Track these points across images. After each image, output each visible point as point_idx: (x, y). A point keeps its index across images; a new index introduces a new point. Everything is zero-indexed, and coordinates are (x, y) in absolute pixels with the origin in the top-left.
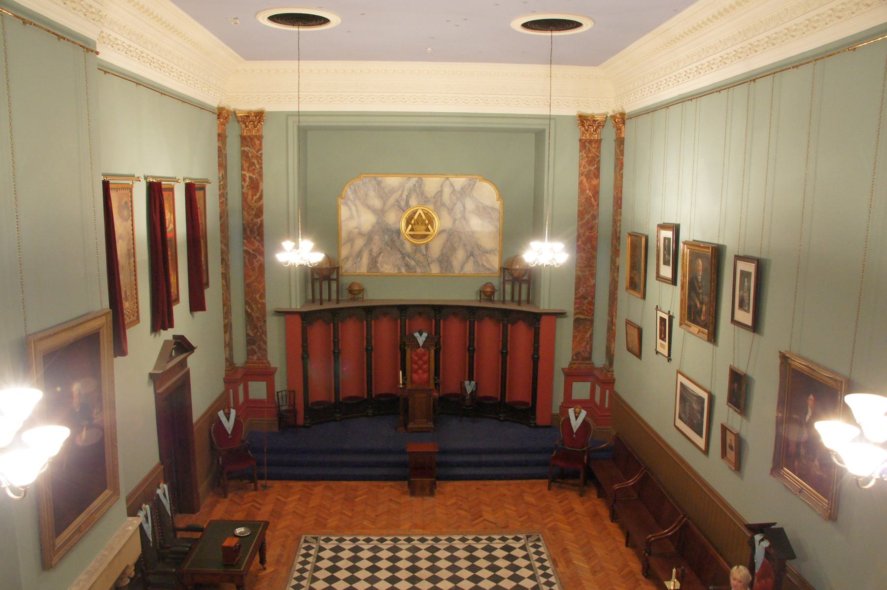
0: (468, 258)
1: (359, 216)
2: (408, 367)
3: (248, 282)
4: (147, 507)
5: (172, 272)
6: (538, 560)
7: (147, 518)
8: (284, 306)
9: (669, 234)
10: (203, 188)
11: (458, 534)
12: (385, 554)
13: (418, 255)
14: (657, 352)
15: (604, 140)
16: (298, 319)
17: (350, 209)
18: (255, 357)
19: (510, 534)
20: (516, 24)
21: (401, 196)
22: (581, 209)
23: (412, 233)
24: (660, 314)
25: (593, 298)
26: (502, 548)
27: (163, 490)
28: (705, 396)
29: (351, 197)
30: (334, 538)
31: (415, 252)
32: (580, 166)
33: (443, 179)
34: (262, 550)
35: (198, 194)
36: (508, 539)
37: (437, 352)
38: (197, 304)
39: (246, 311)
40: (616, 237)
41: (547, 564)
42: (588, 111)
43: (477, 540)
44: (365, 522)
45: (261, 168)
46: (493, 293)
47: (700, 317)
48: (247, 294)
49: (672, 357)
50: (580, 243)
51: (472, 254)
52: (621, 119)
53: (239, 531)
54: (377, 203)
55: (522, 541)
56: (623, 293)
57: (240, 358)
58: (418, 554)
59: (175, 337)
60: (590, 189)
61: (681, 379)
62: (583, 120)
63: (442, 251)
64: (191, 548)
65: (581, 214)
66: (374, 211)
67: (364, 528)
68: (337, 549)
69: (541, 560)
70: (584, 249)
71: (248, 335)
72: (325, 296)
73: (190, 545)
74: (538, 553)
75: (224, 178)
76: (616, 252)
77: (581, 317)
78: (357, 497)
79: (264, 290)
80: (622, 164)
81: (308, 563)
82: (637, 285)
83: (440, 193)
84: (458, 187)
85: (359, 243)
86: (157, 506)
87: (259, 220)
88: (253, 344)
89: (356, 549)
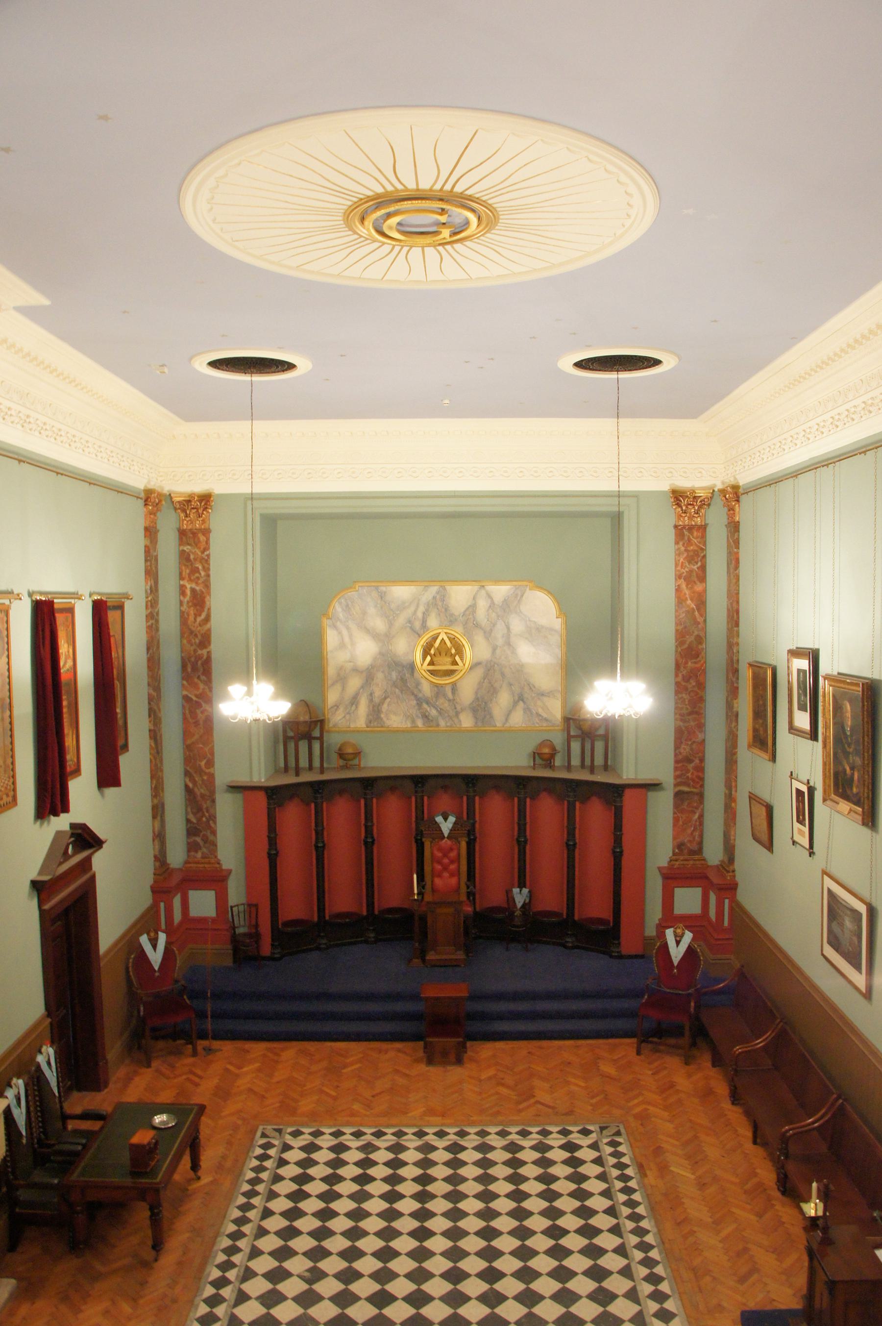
0: (515, 704)
1: (353, 644)
2: (427, 869)
3: (189, 742)
4: (21, 1082)
5: (68, 730)
6: (616, 1166)
7: (18, 1099)
8: (243, 779)
9: (803, 664)
10: (120, 607)
11: (496, 1125)
12: (382, 1156)
14: (794, 843)
15: (709, 526)
16: (262, 796)
17: (340, 633)
18: (199, 855)
19: (575, 1124)
20: (566, 363)
21: (415, 612)
22: (680, 628)
23: (431, 668)
24: (796, 785)
25: (702, 760)
26: (562, 1147)
27: (46, 1057)
28: (862, 909)
29: (341, 616)
30: (307, 1130)
31: (437, 695)
32: (676, 565)
33: (476, 588)
34: (194, 1146)
35: (112, 616)
36: (570, 1132)
37: (471, 845)
38: (108, 776)
39: (186, 786)
40: (733, 670)
41: (629, 1172)
42: (684, 483)
43: (524, 1134)
44: (356, 1106)
45: (208, 576)
46: (552, 756)
47: (852, 789)
48: (188, 760)
49: (815, 850)
50: (680, 679)
52: (733, 495)
53: (158, 1119)
54: (379, 624)
55: (594, 1135)
56: (746, 755)
57: (177, 856)
58: (433, 1156)
59: (73, 826)
60: (692, 600)
61: (829, 883)
62: (678, 496)
63: (476, 693)
64: (84, 1146)
65: (681, 636)
66: (375, 636)
67: (352, 1115)
68: (311, 1148)
69: (621, 1166)
71: (188, 821)
72: (304, 763)
73: (84, 1141)
74: (617, 1154)
75: (153, 591)
76: (733, 691)
77: (686, 789)
78: (345, 1067)
79: (212, 754)
80: (737, 561)
81: (264, 1169)
82: (764, 741)
83: (472, 608)
85: (354, 683)
86: (36, 1081)
87: (204, 652)
89: (340, 1148)
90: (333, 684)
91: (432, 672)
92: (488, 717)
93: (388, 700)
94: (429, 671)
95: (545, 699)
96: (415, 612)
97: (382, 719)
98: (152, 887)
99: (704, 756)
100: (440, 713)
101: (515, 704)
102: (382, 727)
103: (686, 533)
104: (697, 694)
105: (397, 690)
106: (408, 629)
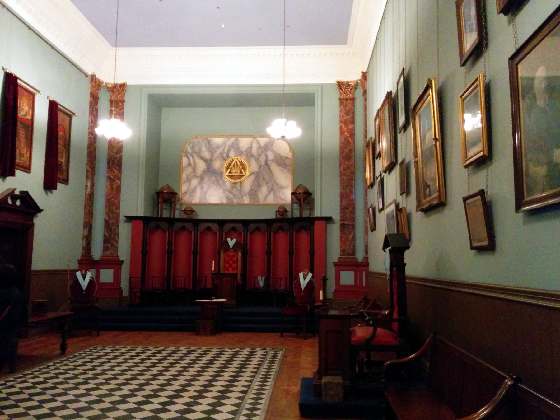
0: (270, 192)
3: (108, 198)
13: (235, 190)
16: (140, 224)
17: (189, 159)
21: (224, 150)
22: (342, 145)
25: (354, 208)
31: (233, 188)
32: (340, 116)
37: (244, 254)
50: (342, 169)
51: (272, 189)
62: (340, 84)
63: (251, 187)
65: (342, 149)
66: (205, 160)
70: (344, 174)
71: (105, 236)
77: (346, 223)
83: (250, 148)
84: (262, 144)
87: (118, 156)
88: (108, 243)
91: (231, 177)
94: (229, 176)
98: (79, 261)
101: (270, 192)
103: (344, 101)
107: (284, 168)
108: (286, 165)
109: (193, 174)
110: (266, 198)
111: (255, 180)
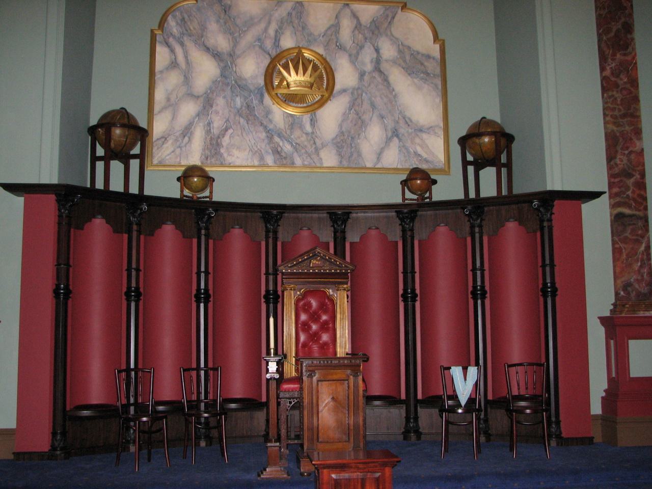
0: (388, 140)
13: (297, 133)
17: (172, 51)
21: (266, 30)
25: (643, 175)
33: (339, 6)
51: (396, 133)
63: (341, 126)
66: (216, 55)
77: (627, 211)
85: (189, 109)
90: (159, 112)
92: (355, 155)
93: (230, 131)
95: (425, 136)
96: (266, 30)
97: (221, 155)
99: (644, 170)
100: (296, 149)
101: (388, 140)
102: (222, 165)
104: (631, 93)
105: (242, 120)
106: (257, 48)
107: (425, 80)
108: (428, 74)
109: (183, 90)
110: (379, 155)
111: (350, 109)
